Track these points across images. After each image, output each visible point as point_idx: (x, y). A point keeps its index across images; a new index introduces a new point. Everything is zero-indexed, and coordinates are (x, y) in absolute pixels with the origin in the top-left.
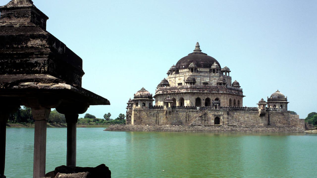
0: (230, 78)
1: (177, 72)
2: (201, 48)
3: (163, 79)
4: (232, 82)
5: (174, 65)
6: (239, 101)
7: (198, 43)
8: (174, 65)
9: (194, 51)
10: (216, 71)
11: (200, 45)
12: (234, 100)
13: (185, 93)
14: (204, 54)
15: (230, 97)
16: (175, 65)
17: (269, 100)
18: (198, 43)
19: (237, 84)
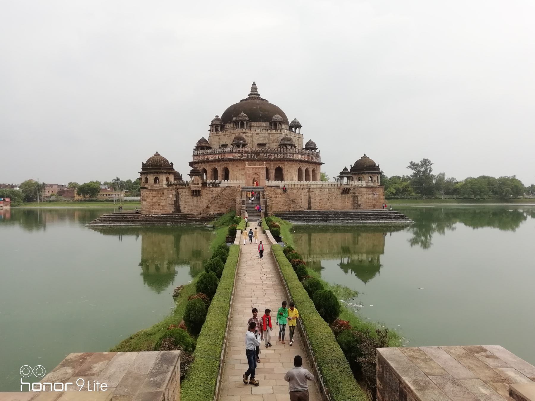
0: (301, 136)
1: (223, 128)
2: (259, 92)
3: (200, 138)
4: (305, 142)
5: (217, 116)
6: (313, 171)
7: (254, 84)
8: (217, 116)
9: (249, 95)
10: (278, 127)
11: (257, 86)
12: (307, 170)
13: (230, 160)
14: (264, 100)
15: (300, 165)
16: (220, 117)
17: (352, 169)
18: (254, 84)
19: (311, 146)
